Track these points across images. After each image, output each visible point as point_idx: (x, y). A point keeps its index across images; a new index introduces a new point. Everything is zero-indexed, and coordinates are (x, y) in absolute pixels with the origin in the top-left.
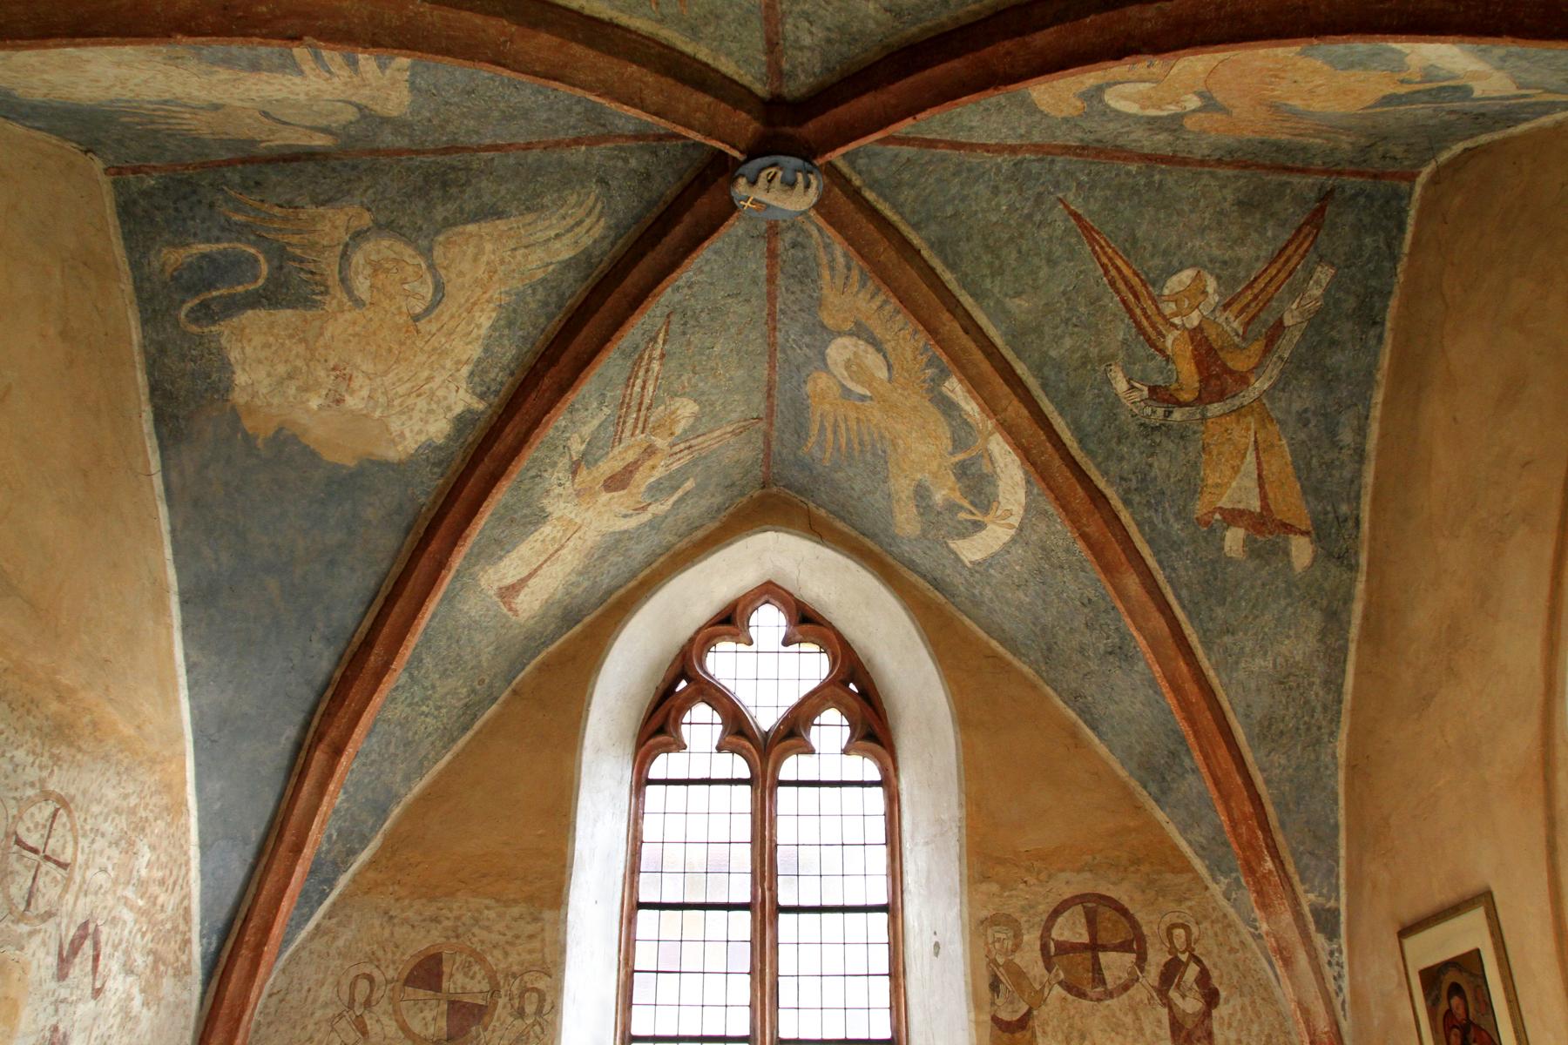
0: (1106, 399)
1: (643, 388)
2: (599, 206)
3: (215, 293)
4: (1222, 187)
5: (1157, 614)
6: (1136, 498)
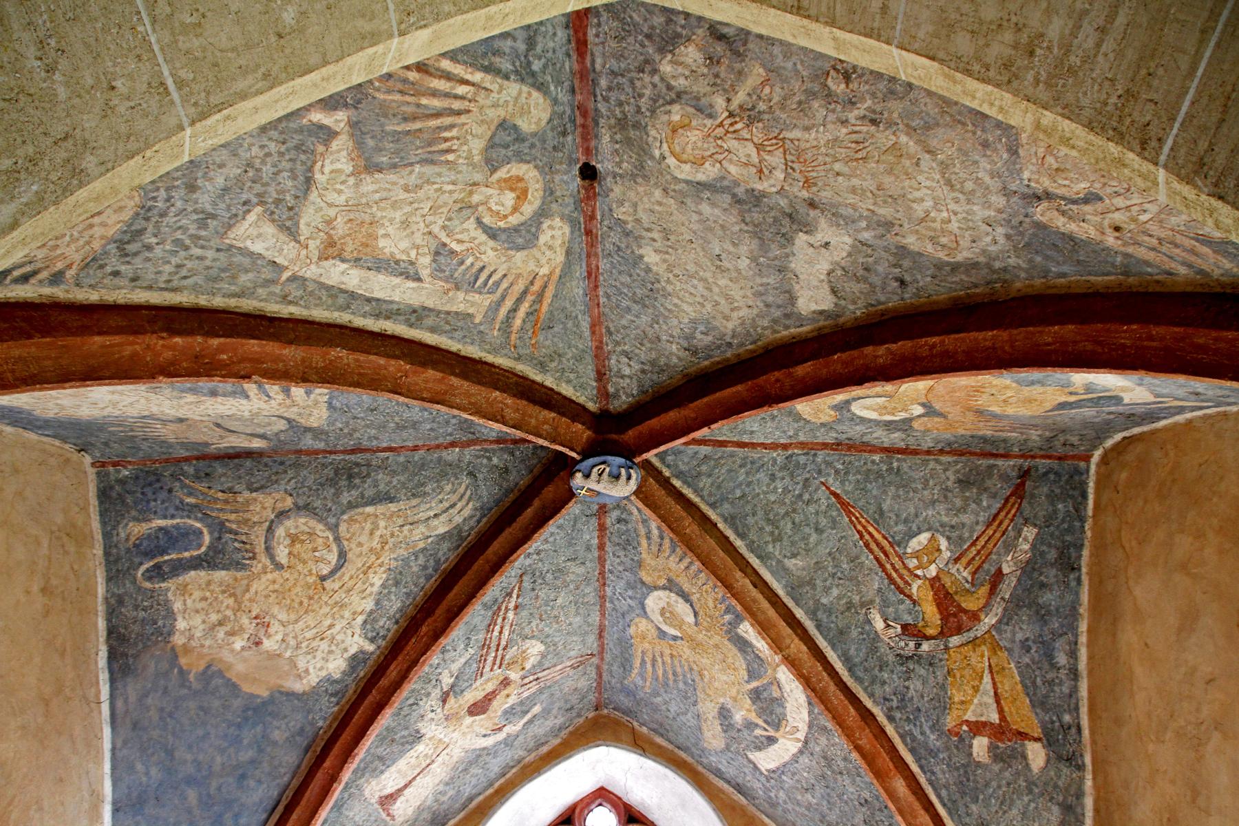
0: (868, 635)
1: (501, 633)
2: (469, 493)
3: (166, 558)
4: (945, 470)
5: (922, 812)
6: (898, 715)
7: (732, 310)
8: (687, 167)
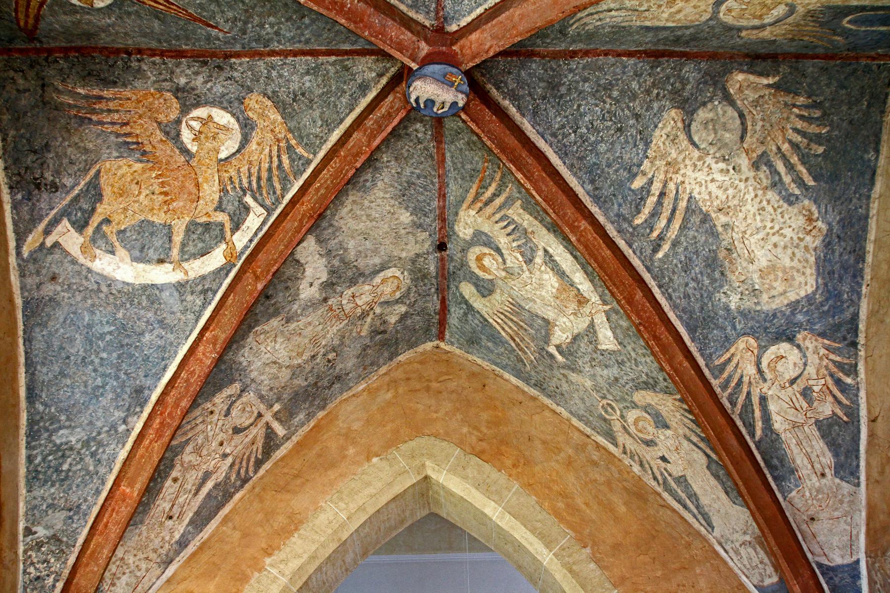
2: (571, 22)
7: (352, 210)
8: (390, 275)
